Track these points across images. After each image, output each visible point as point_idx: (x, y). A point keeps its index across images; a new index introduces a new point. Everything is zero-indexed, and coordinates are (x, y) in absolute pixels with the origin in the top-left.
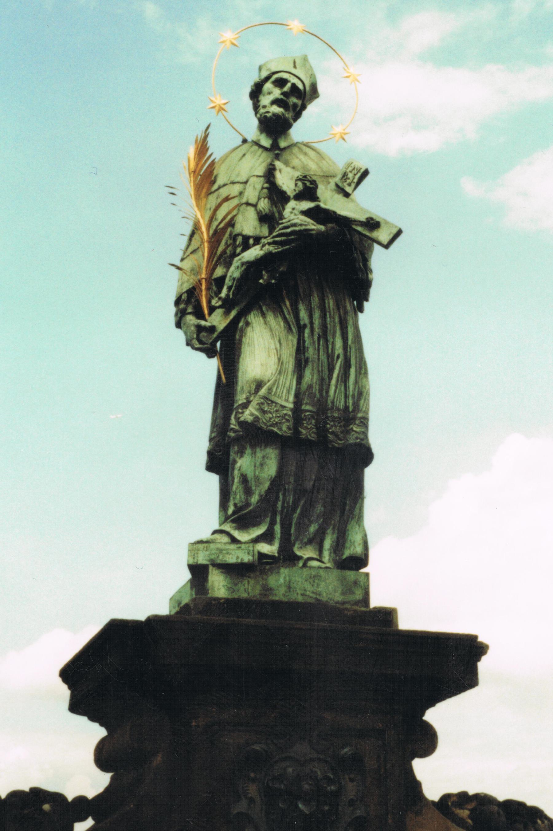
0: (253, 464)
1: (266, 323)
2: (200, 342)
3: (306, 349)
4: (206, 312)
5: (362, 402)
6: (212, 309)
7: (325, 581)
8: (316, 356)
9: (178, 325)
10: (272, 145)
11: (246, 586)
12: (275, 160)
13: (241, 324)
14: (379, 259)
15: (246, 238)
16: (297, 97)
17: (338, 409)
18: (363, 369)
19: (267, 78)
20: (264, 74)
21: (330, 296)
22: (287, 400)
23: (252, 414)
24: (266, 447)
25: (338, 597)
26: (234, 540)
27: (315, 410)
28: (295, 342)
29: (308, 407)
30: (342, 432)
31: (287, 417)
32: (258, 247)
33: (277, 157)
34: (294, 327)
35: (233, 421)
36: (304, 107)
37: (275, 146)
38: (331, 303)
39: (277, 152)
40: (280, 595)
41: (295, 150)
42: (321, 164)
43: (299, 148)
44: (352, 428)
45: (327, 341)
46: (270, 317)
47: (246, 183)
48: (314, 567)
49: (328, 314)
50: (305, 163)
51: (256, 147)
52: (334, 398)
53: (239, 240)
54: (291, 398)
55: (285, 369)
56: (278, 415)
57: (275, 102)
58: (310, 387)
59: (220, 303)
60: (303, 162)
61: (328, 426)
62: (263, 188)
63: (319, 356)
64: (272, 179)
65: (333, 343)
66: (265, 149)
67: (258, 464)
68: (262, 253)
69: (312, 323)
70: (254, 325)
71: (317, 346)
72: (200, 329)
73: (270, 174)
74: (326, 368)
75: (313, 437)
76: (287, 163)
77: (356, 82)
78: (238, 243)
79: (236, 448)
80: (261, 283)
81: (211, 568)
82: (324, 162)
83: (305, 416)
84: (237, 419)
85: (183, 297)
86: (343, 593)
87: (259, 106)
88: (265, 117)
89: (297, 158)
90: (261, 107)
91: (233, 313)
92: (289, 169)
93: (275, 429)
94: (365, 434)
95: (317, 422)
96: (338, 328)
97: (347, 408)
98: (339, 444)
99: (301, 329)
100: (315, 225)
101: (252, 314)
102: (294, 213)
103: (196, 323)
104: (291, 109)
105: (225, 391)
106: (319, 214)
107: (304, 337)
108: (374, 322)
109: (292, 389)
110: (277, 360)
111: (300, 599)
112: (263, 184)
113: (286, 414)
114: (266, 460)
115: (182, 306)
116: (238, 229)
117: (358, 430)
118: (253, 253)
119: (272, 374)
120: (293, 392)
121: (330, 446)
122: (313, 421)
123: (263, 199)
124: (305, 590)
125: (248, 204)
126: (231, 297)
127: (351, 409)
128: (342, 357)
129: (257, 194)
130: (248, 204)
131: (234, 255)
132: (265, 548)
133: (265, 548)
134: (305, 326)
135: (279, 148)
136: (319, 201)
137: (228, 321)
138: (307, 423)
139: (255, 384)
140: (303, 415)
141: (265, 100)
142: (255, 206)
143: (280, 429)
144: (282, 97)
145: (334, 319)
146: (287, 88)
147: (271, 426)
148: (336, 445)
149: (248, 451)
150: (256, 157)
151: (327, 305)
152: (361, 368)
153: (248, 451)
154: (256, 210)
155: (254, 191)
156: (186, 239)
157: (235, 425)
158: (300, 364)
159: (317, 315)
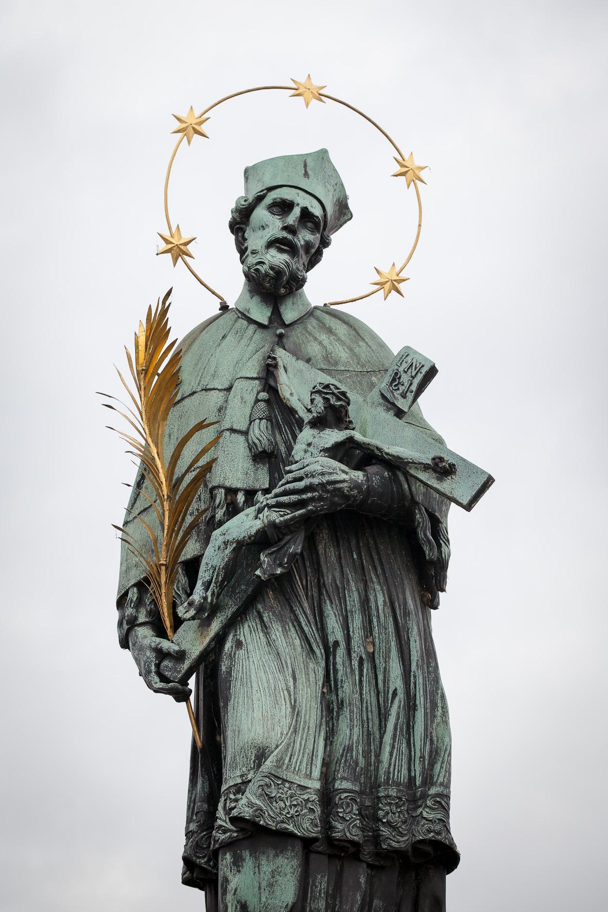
0: (257, 885)
1: (269, 644)
2: (164, 679)
3: (339, 683)
4: (168, 623)
5: (437, 767)
6: (177, 622)
8: (357, 696)
9: (124, 644)
10: (270, 319)
12: (276, 348)
13: (228, 645)
15: (232, 492)
17: (398, 784)
18: (440, 709)
19: (259, 199)
20: (256, 189)
21: (378, 587)
22: (309, 776)
23: (250, 805)
24: (276, 855)
27: (357, 789)
28: (321, 673)
29: (346, 785)
30: (404, 822)
31: (309, 805)
32: (251, 511)
35: (220, 813)
36: (325, 243)
38: (379, 598)
41: (312, 324)
42: (357, 350)
43: (318, 319)
44: (421, 813)
45: (374, 668)
46: (276, 630)
47: (229, 389)
49: (375, 620)
51: (245, 323)
52: (390, 765)
53: (220, 495)
54: (316, 773)
55: (305, 722)
56: (295, 803)
57: (273, 243)
58: (349, 749)
59: (192, 612)
60: (325, 347)
61: (381, 813)
62: (257, 401)
63: (361, 694)
64: (272, 383)
66: (261, 326)
67: (264, 884)
68: (258, 524)
69: (348, 639)
70: (250, 647)
71: (357, 678)
72: (161, 655)
73: (268, 374)
74: (375, 712)
75: (355, 835)
76: (297, 354)
77: (418, 182)
78: (217, 501)
79: (228, 856)
80: (258, 577)
82: (361, 343)
83: (340, 799)
84: (228, 811)
85: (130, 595)
87: (246, 248)
88: (257, 270)
89: (316, 339)
90: (249, 252)
91: (216, 626)
92: (301, 364)
93: (291, 828)
94: (444, 823)
96: (393, 644)
97: (412, 779)
99: (329, 651)
100: (346, 473)
101: (246, 626)
102: (312, 456)
103: (153, 645)
104: (302, 252)
105: (208, 757)
106: (351, 453)
107: (335, 664)
108: (457, 626)
109: (317, 757)
110: (289, 709)
112: (258, 394)
113: (307, 801)
115: (129, 611)
116: (217, 477)
117: (431, 817)
118: (245, 524)
119: (282, 734)
120: (318, 762)
121: (385, 847)
122: (355, 807)
123: (257, 421)
125: (232, 430)
126: (209, 600)
128: (401, 695)
129: (248, 411)
130: (232, 430)
131: (213, 524)
134: (336, 643)
135: (284, 325)
136: (353, 429)
137: (207, 640)
139: (254, 752)
140: (337, 799)
141: (256, 240)
142: (245, 433)
144: (285, 234)
149: (248, 863)
151: (373, 605)
152: (434, 706)
154: (247, 440)
155: (242, 405)
156: (129, 492)
157: (225, 821)
158: (331, 709)
159: (356, 622)
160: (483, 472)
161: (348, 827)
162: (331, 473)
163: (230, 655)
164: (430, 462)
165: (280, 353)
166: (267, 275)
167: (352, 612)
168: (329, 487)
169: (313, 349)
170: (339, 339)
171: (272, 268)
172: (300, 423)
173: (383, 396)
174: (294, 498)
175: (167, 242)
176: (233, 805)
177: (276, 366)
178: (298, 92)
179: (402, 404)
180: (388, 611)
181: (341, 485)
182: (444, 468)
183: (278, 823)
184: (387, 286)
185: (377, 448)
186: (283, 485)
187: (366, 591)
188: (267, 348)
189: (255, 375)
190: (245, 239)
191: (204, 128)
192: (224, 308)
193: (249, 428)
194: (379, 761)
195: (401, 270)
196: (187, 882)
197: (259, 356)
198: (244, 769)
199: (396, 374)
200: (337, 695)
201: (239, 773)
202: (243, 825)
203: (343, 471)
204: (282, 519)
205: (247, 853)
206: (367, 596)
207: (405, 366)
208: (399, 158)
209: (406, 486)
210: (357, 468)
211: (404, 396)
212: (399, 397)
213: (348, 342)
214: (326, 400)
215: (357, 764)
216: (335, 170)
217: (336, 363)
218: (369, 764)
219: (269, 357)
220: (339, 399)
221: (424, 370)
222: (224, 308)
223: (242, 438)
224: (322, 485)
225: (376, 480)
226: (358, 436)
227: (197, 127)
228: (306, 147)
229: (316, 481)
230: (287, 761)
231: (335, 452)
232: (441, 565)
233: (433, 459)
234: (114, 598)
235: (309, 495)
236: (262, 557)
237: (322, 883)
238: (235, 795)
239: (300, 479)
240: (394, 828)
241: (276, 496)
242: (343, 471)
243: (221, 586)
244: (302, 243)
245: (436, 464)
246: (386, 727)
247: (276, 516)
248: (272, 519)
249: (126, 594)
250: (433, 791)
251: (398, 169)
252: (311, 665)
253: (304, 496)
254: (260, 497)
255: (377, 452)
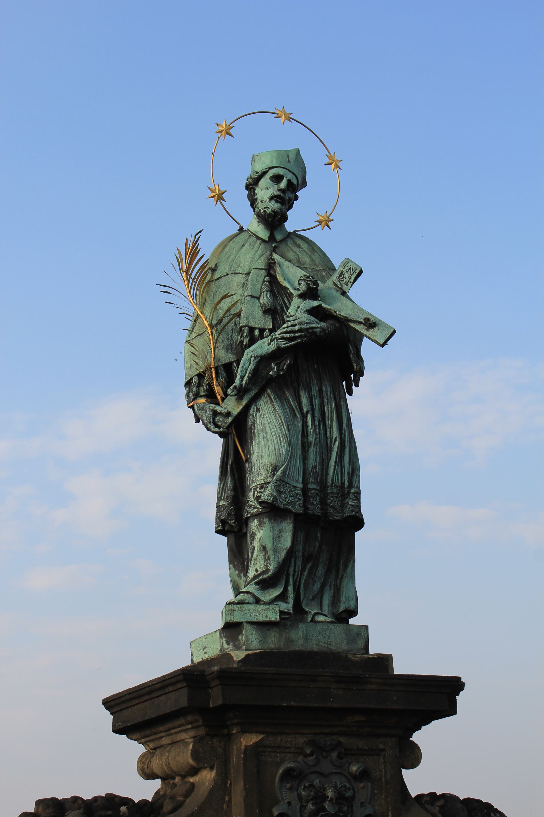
0: (271, 536)
2: (217, 426)
5: (355, 478)
7: (334, 633)
10: (269, 238)
11: (273, 639)
12: (273, 253)
13: (251, 411)
14: (368, 349)
15: (252, 330)
16: (290, 190)
19: (264, 173)
21: (328, 383)
22: (297, 481)
24: (282, 522)
25: (344, 646)
26: (258, 601)
27: (318, 488)
30: (340, 506)
33: (274, 250)
34: (299, 413)
37: (272, 238)
38: (327, 389)
39: (274, 245)
40: (299, 645)
41: (290, 242)
42: (314, 257)
44: (348, 502)
45: (325, 425)
47: (248, 274)
48: (322, 622)
50: (300, 255)
53: (246, 331)
54: (301, 480)
58: (315, 467)
59: (235, 392)
60: (298, 255)
61: (329, 501)
62: (264, 281)
64: (272, 272)
65: (331, 427)
66: (263, 241)
67: (275, 536)
69: (313, 409)
75: (318, 512)
78: (245, 334)
79: (256, 521)
80: (271, 375)
81: (245, 624)
82: (316, 254)
85: (194, 380)
86: (348, 643)
87: (256, 199)
88: (265, 211)
89: (292, 250)
90: (259, 200)
93: (290, 508)
94: (359, 507)
95: (321, 498)
97: (343, 484)
98: (338, 516)
107: (307, 422)
111: (315, 648)
112: (265, 277)
113: (297, 494)
114: (282, 533)
118: (264, 346)
124: (319, 641)
126: (243, 386)
127: (346, 486)
129: (259, 286)
130: (252, 296)
132: (283, 606)
133: (283, 606)
134: (307, 412)
137: (241, 407)
138: (313, 500)
140: (309, 493)
143: (294, 507)
145: (331, 405)
146: (283, 184)
147: (286, 505)
148: (335, 517)
150: (255, 248)
151: (324, 392)
153: (267, 524)
158: (305, 446)
159: (316, 402)
160: (391, 328)
161: (315, 509)
162: (311, 323)
163: (253, 415)
164: (363, 321)
165: (276, 256)
166: (270, 214)
167: (314, 396)
168: (310, 331)
169: (291, 255)
170: (304, 251)
171: (273, 211)
172: (290, 296)
173: (334, 283)
174: (292, 335)
175: (212, 191)
176: (259, 494)
177: (275, 263)
178: (278, 116)
179: (345, 288)
180: (332, 396)
181: (316, 330)
182: (371, 324)
183: (284, 505)
184: (323, 223)
185: (335, 312)
186: (285, 328)
187: (321, 385)
188: (268, 253)
189: (263, 268)
190: (255, 194)
191: (232, 131)
192: (241, 230)
193: (260, 296)
194: (327, 474)
195: (330, 215)
196: (217, 532)
197: (264, 257)
198: (265, 476)
199: (342, 273)
200: (308, 439)
201: (262, 478)
202: (265, 505)
203: (317, 323)
204: (284, 346)
205: (267, 519)
206: (321, 388)
207: (346, 268)
208: (328, 154)
209: (346, 332)
210: (321, 320)
211: (347, 285)
212: (344, 285)
213: (309, 253)
214: (308, 285)
215: (318, 475)
216: (302, 160)
217: (304, 264)
218: (322, 475)
219: (271, 258)
220: (314, 284)
221: (358, 271)
222: (241, 230)
223: (257, 301)
224: (307, 329)
225: (333, 327)
226: (324, 305)
227: (228, 131)
228: (290, 146)
229: (303, 327)
230: (287, 473)
231: (312, 312)
232: (360, 373)
233: (365, 319)
234: (184, 382)
235: (299, 334)
236: (273, 365)
237: (301, 537)
238: (260, 489)
239: (295, 325)
240: (336, 509)
241: (281, 333)
242: (317, 323)
243: (250, 378)
244: (287, 198)
245: (366, 322)
246: (331, 456)
247: (283, 344)
248: (279, 345)
249: (192, 379)
250: (353, 491)
251: (327, 161)
252: (296, 423)
253: (297, 335)
254: (267, 333)
255: (334, 314)
